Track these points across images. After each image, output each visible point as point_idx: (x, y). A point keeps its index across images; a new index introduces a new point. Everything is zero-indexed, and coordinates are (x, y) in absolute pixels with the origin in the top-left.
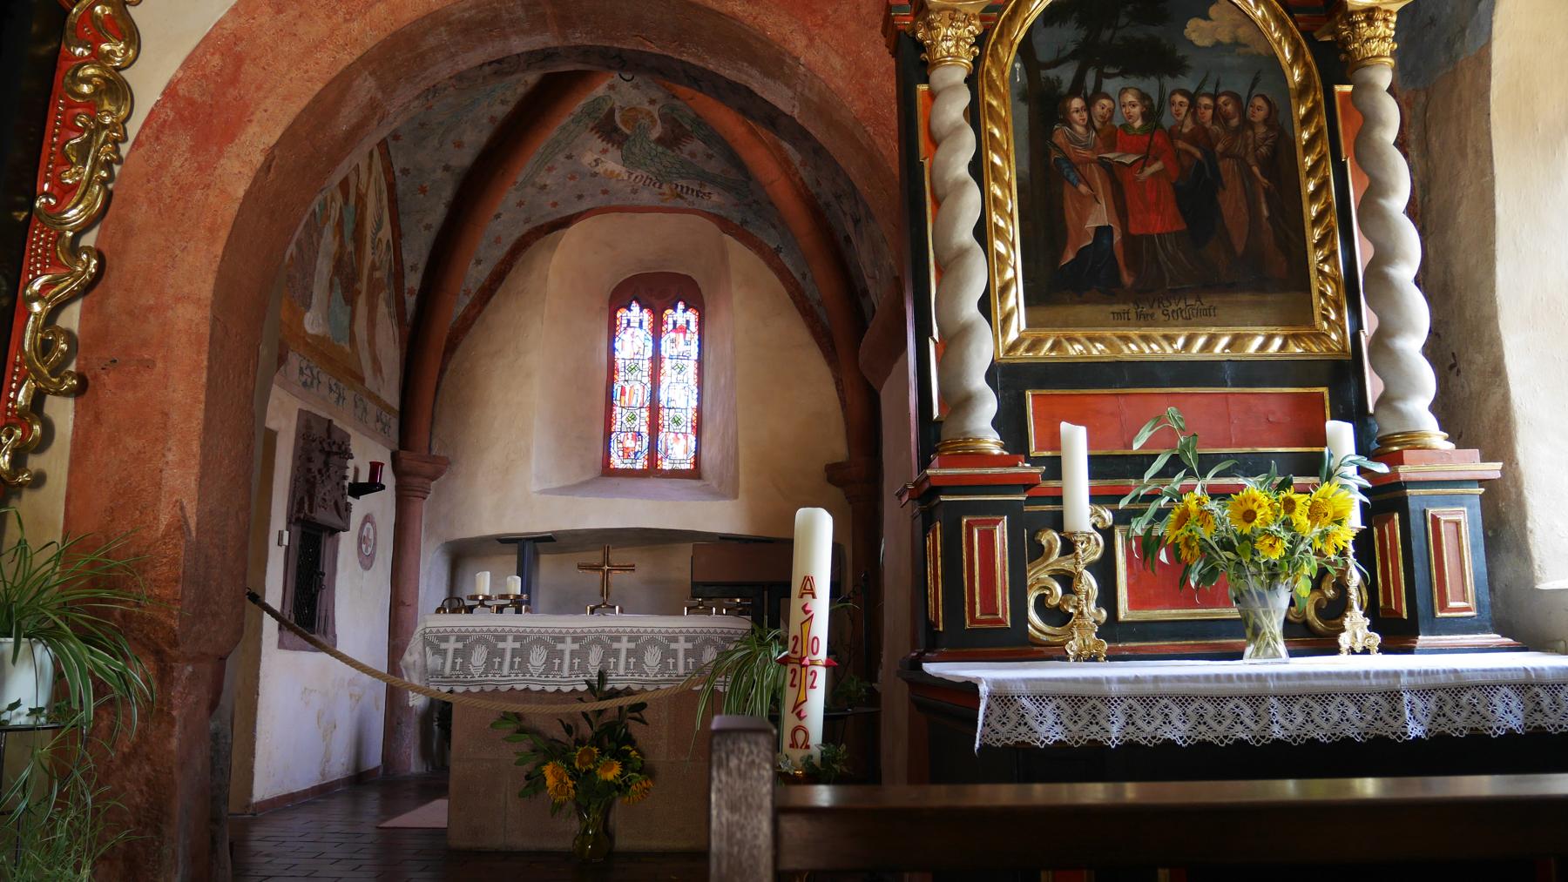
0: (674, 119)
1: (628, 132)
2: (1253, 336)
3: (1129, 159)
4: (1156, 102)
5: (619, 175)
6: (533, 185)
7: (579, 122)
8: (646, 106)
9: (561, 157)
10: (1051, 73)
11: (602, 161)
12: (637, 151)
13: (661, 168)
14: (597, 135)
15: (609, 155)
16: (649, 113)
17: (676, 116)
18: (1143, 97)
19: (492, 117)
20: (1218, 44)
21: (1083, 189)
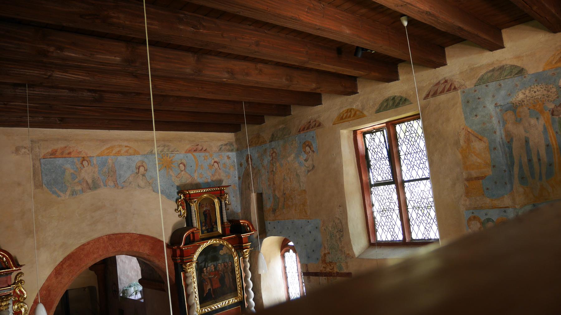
2: (231, 300)
3: (212, 277)
4: (216, 265)
10: (201, 265)
18: (214, 265)
20: (224, 254)
21: (206, 283)
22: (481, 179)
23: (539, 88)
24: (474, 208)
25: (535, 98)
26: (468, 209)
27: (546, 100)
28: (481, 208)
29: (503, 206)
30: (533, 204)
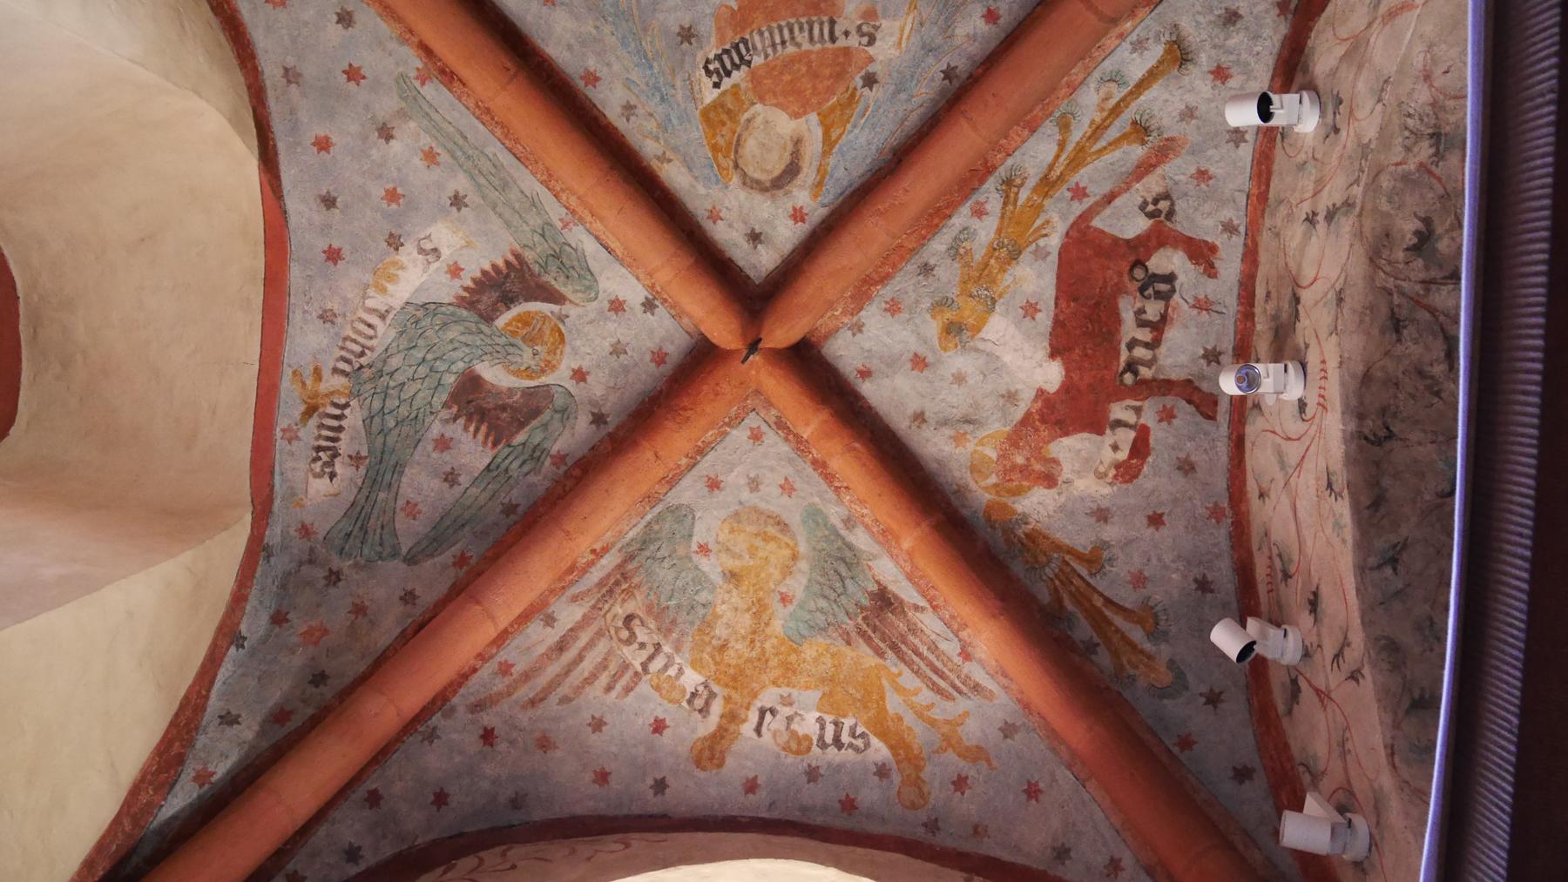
0: (536, 413)
1: (502, 321)
5: (384, 290)
6: (403, 115)
7: (543, 236)
8: (567, 364)
9: (461, 183)
11: (429, 263)
12: (451, 335)
13: (400, 378)
14: (500, 263)
15: (445, 278)
16: (549, 367)
17: (545, 416)
19: (597, 79)
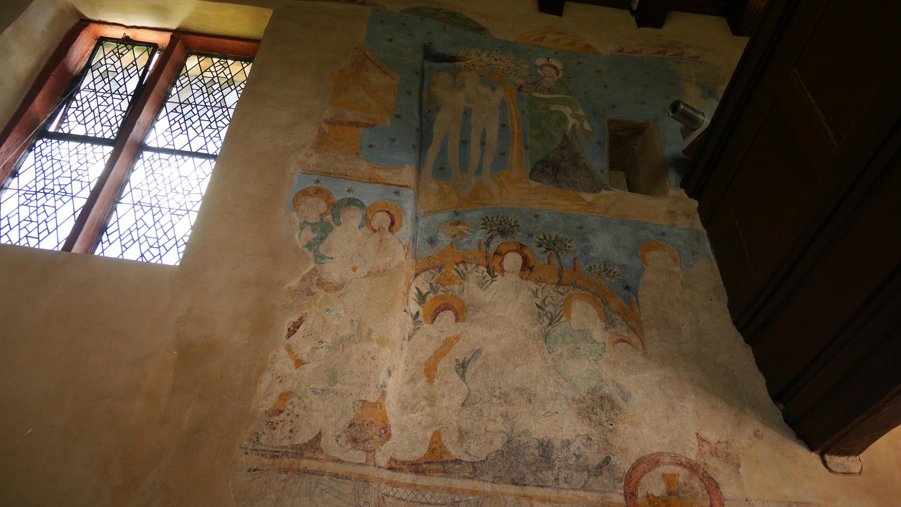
22: (363, 127)
23: (503, 57)
24: (325, 173)
25: (495, 67)
26: (308, 172)
27: (511, 73)
28: (343, 176)
29: (396, 183)
30: (455, 212)
